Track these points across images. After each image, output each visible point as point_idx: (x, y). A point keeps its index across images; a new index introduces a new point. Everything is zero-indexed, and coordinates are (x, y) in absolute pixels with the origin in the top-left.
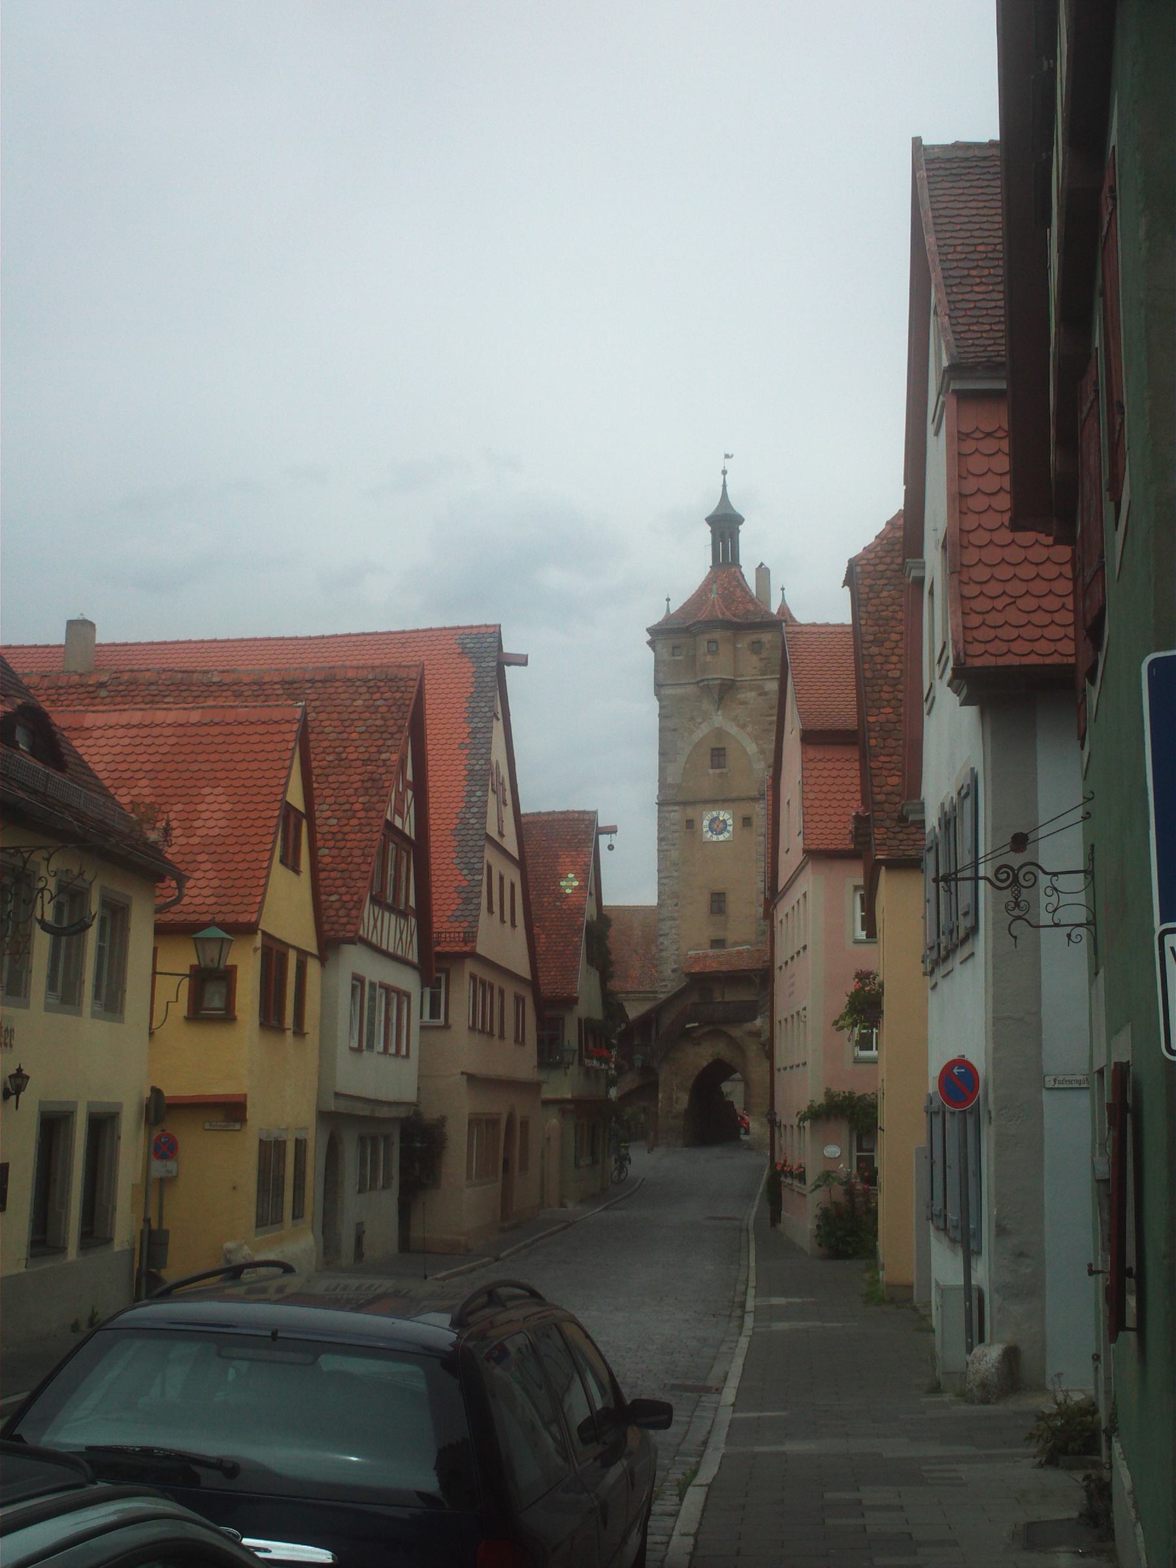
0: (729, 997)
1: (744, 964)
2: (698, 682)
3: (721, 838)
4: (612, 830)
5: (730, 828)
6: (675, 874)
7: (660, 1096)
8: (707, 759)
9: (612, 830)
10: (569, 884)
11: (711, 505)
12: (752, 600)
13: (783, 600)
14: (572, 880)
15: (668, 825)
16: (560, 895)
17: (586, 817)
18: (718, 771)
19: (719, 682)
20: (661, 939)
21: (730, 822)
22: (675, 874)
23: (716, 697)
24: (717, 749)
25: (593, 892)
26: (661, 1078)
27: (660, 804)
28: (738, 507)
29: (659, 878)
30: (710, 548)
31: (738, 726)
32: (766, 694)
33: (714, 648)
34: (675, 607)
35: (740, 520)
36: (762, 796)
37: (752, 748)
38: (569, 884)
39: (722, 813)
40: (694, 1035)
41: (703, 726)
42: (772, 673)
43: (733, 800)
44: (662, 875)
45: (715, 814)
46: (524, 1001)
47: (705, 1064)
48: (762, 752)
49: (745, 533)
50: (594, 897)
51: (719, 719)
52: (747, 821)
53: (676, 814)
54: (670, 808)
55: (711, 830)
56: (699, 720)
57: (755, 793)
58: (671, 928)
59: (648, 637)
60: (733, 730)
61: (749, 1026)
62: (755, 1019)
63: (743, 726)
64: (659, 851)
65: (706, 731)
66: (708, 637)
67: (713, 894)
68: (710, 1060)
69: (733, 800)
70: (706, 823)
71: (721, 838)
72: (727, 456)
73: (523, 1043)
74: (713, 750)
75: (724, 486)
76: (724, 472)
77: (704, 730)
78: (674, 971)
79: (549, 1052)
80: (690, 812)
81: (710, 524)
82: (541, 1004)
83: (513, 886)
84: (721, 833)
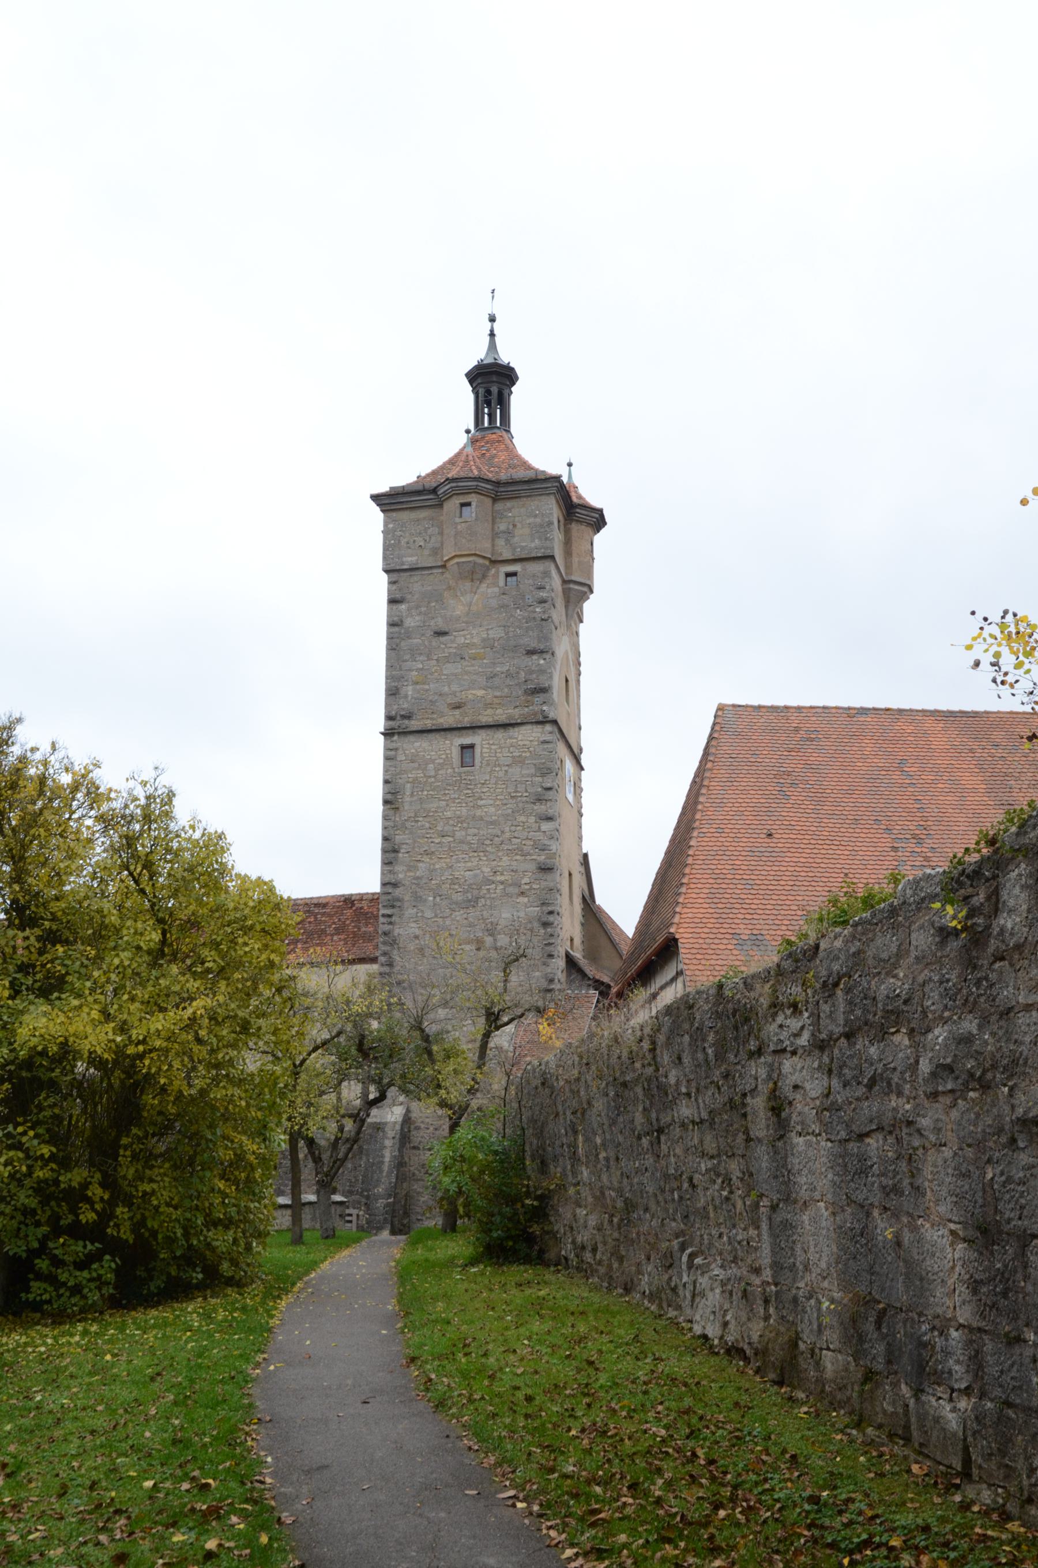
27: (388, 734)
75: (492, 335)
76: (492, 319)
81: (471, 382)
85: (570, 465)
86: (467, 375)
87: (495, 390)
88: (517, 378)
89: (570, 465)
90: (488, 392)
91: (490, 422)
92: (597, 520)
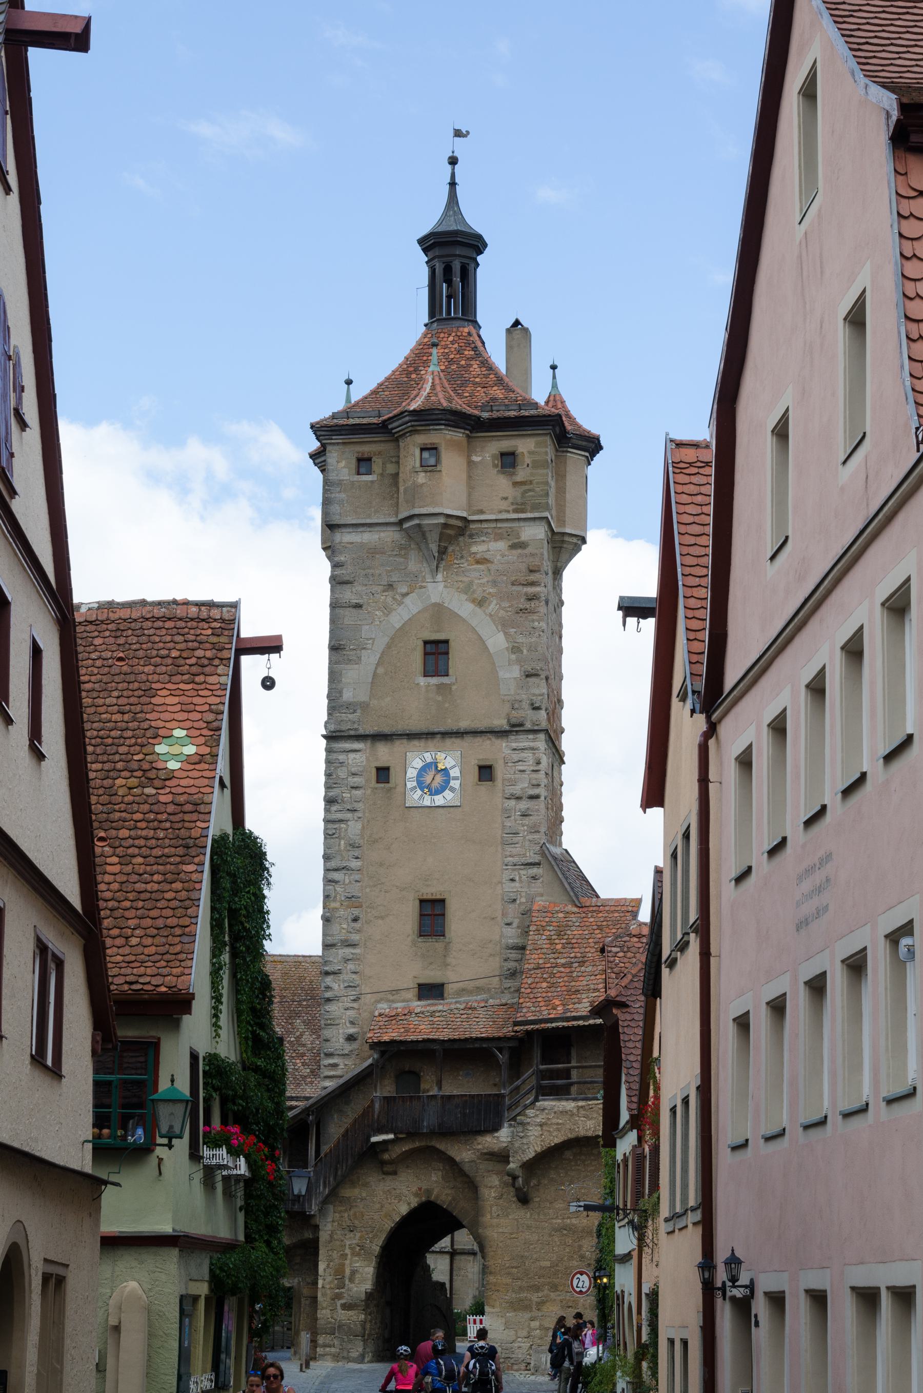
0: (452, 1088)
1: (481, 1026)
2: (401, 522)
3: (439, 800)
4: (270, 646)
5: (456, 784)
6: (355, 864)
7: (322, 1266)
8: (417, 658)
9: (270, 646)
10: (176, 750)
11: (428, 220)
12: (499, 380)
13: (555, 386)
14: (180, 742)
15: (342, 773)
16: (153, 774)
17: (215, 613)
18: (434, 681)
19: (442, 520)
20: (329, 980)
21: (455, 772)
22: (355, 864)
23: (434, 547)
24: (436, 642)
25: (227, 781)
26: (324, 1236)
27: (330, 738)
28: (476, 218)
29: (327, 870)
30: (426, 290)
31: (473, 601)
32: (522, 545)
33: (432, 461)
34: (359, 392)
35: (477, 244)
36: (515, 728)
37: (497, 641)
38: (176, 750)
39: (441, 756)
40: (386, 1157)
41: (408, 600)
42: (535, 508)
43: (459, 734)
45: (428, 757)
46: (60, 964)
47: (404, 1210)
48: (516, 649)
49: (489, 272)
50: (227, 792)
51: (437, 589)
52: (486, 772)
56: (404, 590)
57: (501, 723)
58: (347, 960)
59: (315, 445)
60: (464, 608)
61: (488, 1142)
62: (496, 1128)
63: (481, 603)
64: (327, 821)
66: (422, 439)
67: (422, 901)
68: (415, 1202)
69: (459, 734)
70: (412, 773)
71: (439, 800)
72: (458, 134)
73: (56, 1072)
74: (426, 643)
76: (453, 161)
77: (412, 606)
78: (351, 1038)
79: (124, 1114)
80: (384, 754)
81: (426, 251)
82: (108, 1009)
83: (37, 652)
84: (438, 792)
85: (554, 367)
86: (421, 241)
87: (456, 266)
89: (554, 367)
90: (448, 270)
91: (449, 312)
92: (591, 446)
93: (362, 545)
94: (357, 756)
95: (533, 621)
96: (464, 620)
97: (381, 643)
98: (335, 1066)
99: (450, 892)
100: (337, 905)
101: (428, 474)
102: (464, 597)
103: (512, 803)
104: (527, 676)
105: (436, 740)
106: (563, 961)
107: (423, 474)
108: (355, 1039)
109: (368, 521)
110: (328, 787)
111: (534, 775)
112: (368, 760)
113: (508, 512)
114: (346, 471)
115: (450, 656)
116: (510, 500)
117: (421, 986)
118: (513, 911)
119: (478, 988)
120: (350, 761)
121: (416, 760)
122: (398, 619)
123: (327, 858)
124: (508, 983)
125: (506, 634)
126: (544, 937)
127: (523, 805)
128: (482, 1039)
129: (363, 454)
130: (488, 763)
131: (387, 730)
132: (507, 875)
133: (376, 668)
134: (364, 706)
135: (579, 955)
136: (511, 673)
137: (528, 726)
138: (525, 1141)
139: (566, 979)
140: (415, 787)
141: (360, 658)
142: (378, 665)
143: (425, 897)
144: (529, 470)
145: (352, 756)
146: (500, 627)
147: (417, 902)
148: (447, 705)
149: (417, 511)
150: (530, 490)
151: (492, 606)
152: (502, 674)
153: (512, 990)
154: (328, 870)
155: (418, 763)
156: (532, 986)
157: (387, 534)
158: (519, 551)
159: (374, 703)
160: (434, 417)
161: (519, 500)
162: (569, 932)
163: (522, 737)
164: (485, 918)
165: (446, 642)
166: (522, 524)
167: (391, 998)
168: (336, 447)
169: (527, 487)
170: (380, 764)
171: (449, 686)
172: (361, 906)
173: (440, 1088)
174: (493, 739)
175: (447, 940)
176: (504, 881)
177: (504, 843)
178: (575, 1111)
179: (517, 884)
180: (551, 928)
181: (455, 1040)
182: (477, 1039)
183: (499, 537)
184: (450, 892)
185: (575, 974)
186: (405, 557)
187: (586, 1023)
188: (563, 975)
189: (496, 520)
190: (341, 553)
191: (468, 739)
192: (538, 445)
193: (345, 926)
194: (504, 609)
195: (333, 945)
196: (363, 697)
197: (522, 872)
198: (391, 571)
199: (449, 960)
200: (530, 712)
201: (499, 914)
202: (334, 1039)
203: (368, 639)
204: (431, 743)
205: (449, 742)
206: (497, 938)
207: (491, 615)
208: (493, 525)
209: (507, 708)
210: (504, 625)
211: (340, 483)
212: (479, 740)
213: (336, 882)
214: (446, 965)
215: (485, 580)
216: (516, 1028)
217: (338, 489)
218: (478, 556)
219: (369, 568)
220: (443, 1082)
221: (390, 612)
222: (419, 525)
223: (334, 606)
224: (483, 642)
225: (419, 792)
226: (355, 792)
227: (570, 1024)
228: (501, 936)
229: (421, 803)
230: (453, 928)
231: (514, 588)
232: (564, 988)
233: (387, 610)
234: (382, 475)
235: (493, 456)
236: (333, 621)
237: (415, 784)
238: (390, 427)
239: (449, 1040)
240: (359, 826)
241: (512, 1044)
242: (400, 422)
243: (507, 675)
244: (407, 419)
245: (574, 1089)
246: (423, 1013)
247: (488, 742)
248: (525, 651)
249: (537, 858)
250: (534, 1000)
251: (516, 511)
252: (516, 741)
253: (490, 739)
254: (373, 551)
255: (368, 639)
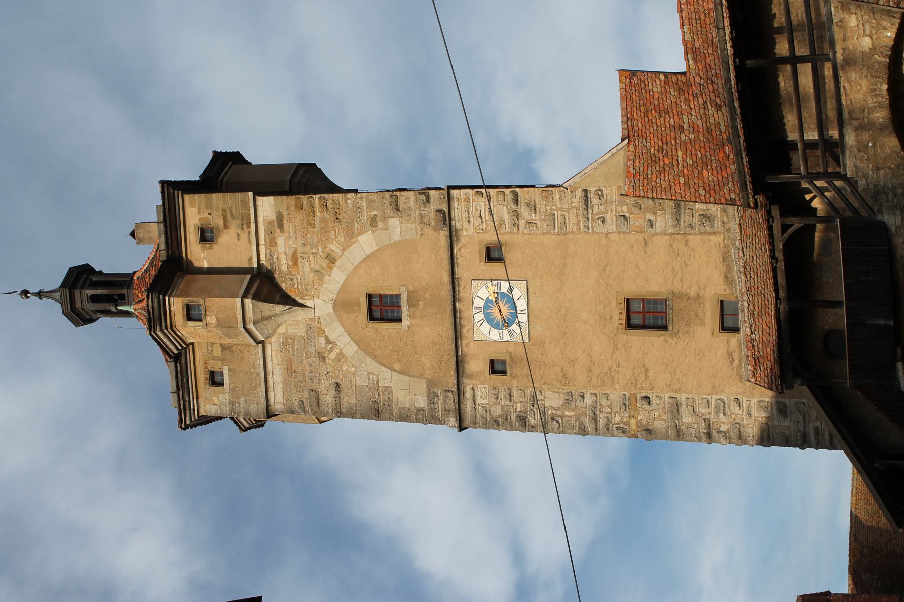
2: (258, 342)
18: (405, 309)
19: (248, 302)
22: (589, 400)
23: (279, 308)
32: (280, 217)
37: (366, 243)
39: (479, 303)
41: (332, 337)
44: (590, 426)
45: (479, 316)
51: (321, 305)
53: (482, 393)
54: (468, 406)
55: (507, 323)
56: (323, 340)
60: (337, 278)
62: (883, 228)
63: (331, 260)
65: (341, 329)
70: (495, 335)
71: (521, 305)
74: (372, 318)
75: (40, 295)
77: (336, 332)
80: (476, 365)
88: (87, 265)
93: (285, 383)
94: (478, 394)
95: (346, 204)
96: (348, 278)
97: (372, 365)
98: (816, 430)
99: (617, 293)
100: (633, 422)
101: (208, 313)
102: (327, 278)
103: (522, 223)
104: (398, 210)
105: (461, 307)
106: (680, 153)
107: (208, 318)
108: (786, 406)
109: (262, 376)
110: (511, 428)
111: (493, 200)
112: (483, 383)
113: (249, 233)
114: (221, 396)
115: (382, 293)
116: (239, 231)
117: (724, 329)
118: (638, 220)
119: (724, 260)
120: (485, 401)
121: (482, 332)
122: (351, 349)
123: (583, 432)
124: (717, 225)
125: (360, 234)
126: (658, 181)
127: (524, 211)
128: (773, 250)
129: (206, 379)
130: (484, 252)
131: (453, 360)
132: (599, 228)
133: (395, 371)
134: (432, 384)
135: (673, 134)
136: (397, 229)
137: (445, 207)
138: (900, 191)
139: (697, 147)
140: (509, 331)
141: (387, 388)
142: (392, 369)
143: (624, 321)
144: (214, 213)
145: (479, 401)
146: (353, 240)
147: (630, 331)
148: (428, 296)
149: (240, 325)
150: (231, 211)
151: (335, 249)
152: (397, 238)
153: (725, 219)
154: (596, 430)
155: (486, 327)
156: (707, 188)
157: (274, 357)
158: (285, 221)
159: (428, 374)
160: (156, 305)
161: (238, 222)
162: (652, 151)
163: (455, 214)
164: (645, 253)
165: (370, 297)
166: (260, 219)
167: (736, 362)
168: (202, 406)
169: (229, 217)
170: (487, 370)
171: (410, 294)
172: (635, 394)
173: (839, 304)
174: (460, 245)
175: (670, 296)
176: (605, 231)
177: (563, 232)
178: (855, 123)
179: (608, 217)
180: (649, 172)
181: (776, 284)
182: (773, 257)
183: (273, 243)
184: (617, 293)
185: (692, 136)
186: (293, 338)
187: (738, 111)
188: (693, 152)
189: (258, 245)
190: (293, 405)
191: (459, 272)
192: (192, 205)
193: (657, 414)
194: (336, 237)
195: (678, 429)
196: (423, 387)
197: (596, 210)
198: (307, 354)
199: (692, 294)
200: (433, 206)
201: (640, 237)
202: (787, 432)
203: (369, 379)
204: (465, 314)
205: (462, 293)
206: (667, 237)
207: (343, 250)
208: (262, 249)
209: (428, 231)
210: (351, 235)
211: (231, 403)
212: (459, 260)
213: (609, 422)
214: (698, 297)
215: (312, 257)
216: (752, 204)
217: (237, 405)
218: (291, 264)
219: (304, 376)
220: (828, 298)
221: (343, 356)
222: (255, 323)
223: (340, 414)
224: (368, 257)
225: (514, 327)
226: (515, 399)
227: (741, 133)
228: (666, 234)
229: (525, 326)
230: (657, 290)
231: (317, 226)
232: (707, 147)
233: (341, 356)
234: (223, 360)
235: (203, 249)
236: (353, 415)
237: (505, 332)
238: (176, 352)
239: (776, 290)
240: (548, 394)
241: (776, 211)
242: (165, 340)
243: (398, 231)
244: (159, 333)
245: (834, 134)
246: (751, 325)
247: (462, 251)
248: (375, 212)
249: (579, 193)
250: (721, 184)
251: (249, 226)
252: (460, 221)
253: (460, 249)
254: (290, 371)
255: (369, 379)
